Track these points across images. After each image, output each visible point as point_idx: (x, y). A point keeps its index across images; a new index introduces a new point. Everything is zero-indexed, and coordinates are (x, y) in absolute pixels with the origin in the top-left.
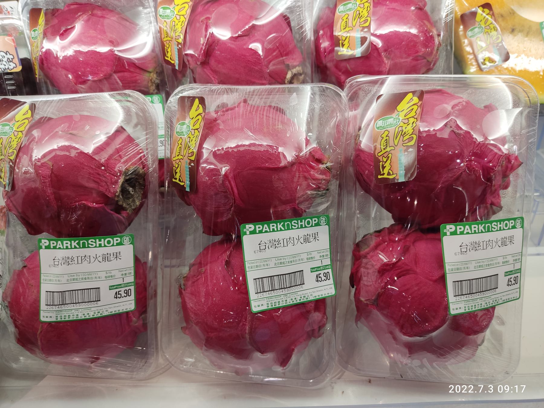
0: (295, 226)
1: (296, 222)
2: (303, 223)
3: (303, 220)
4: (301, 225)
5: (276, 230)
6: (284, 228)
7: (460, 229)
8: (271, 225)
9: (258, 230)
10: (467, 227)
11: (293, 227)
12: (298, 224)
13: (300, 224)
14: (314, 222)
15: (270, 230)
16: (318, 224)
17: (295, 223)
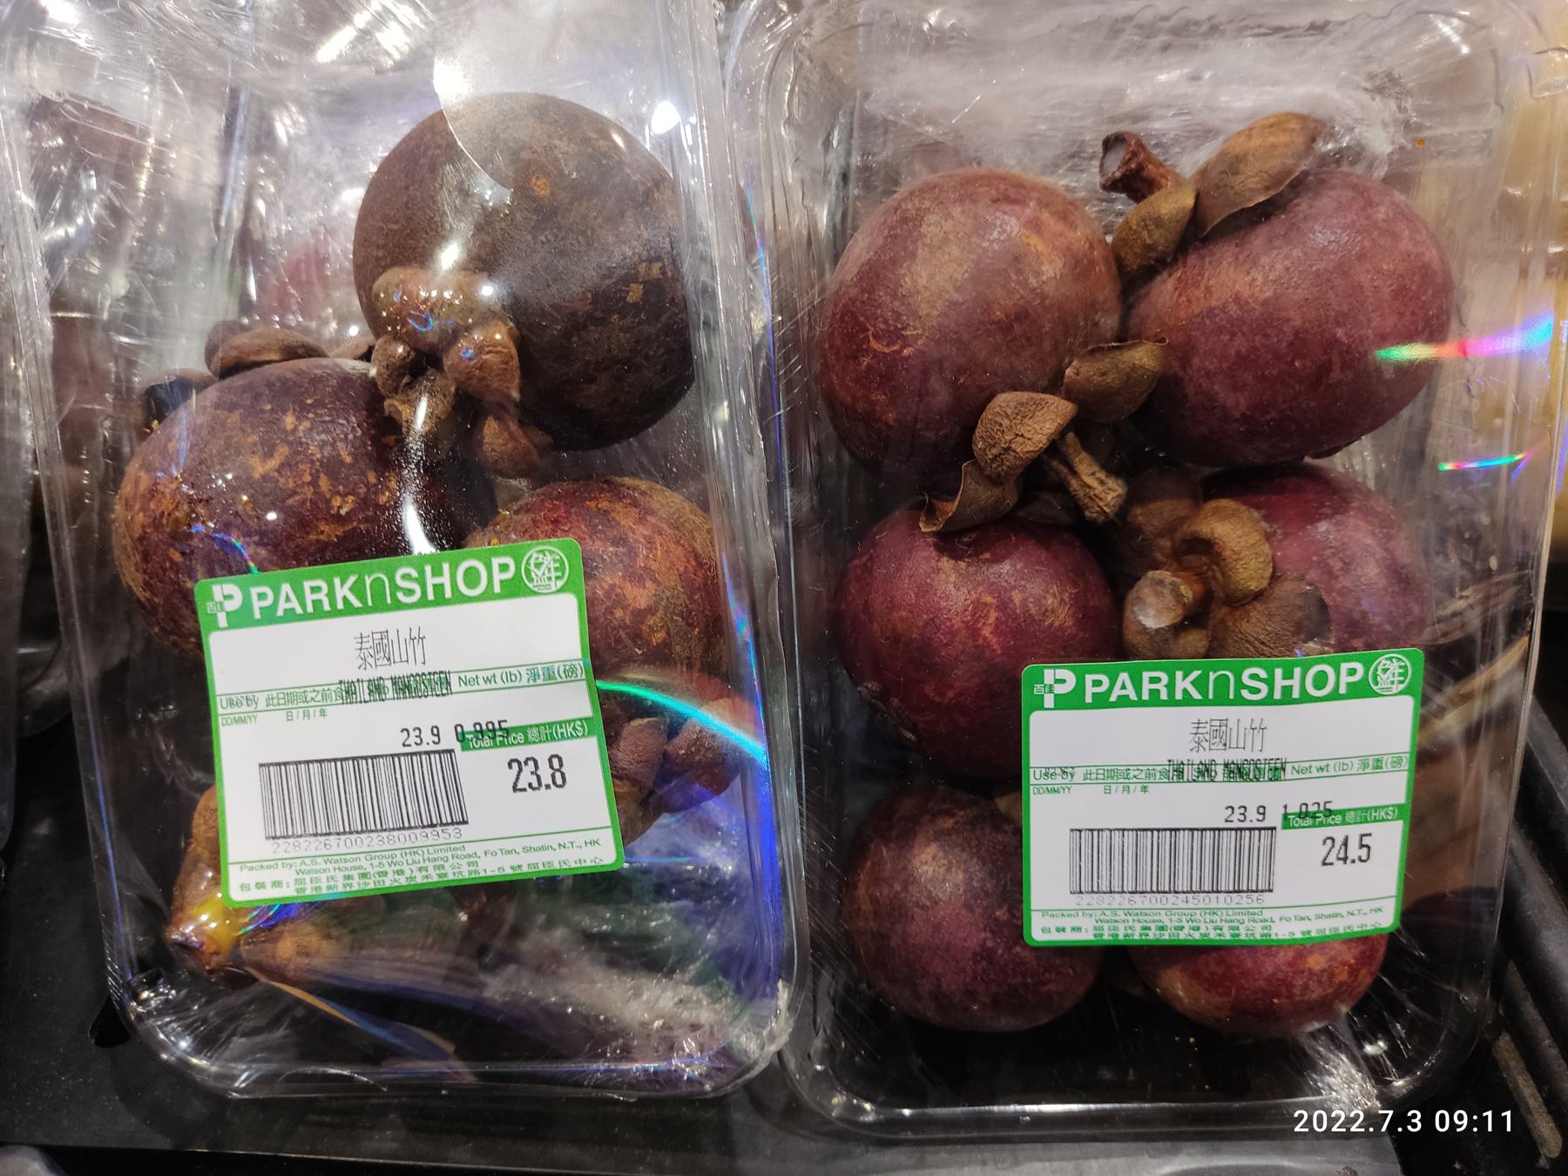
0: (410, 592)
1: (414, 574)
2: (445, 579)
3: (446, 567)
4: (439, 588)
5: (327, 607)
6: (362, 598)
7: (1097, 683)
8: (307, 585)
9: (257, 605)
10: (1124, 677)
11: (400, 596)
12: (422, 582)
13: (431, 581)
14: (498, 576)
15: (303, 605)
16: (515, 588)
17: (406, 577)
